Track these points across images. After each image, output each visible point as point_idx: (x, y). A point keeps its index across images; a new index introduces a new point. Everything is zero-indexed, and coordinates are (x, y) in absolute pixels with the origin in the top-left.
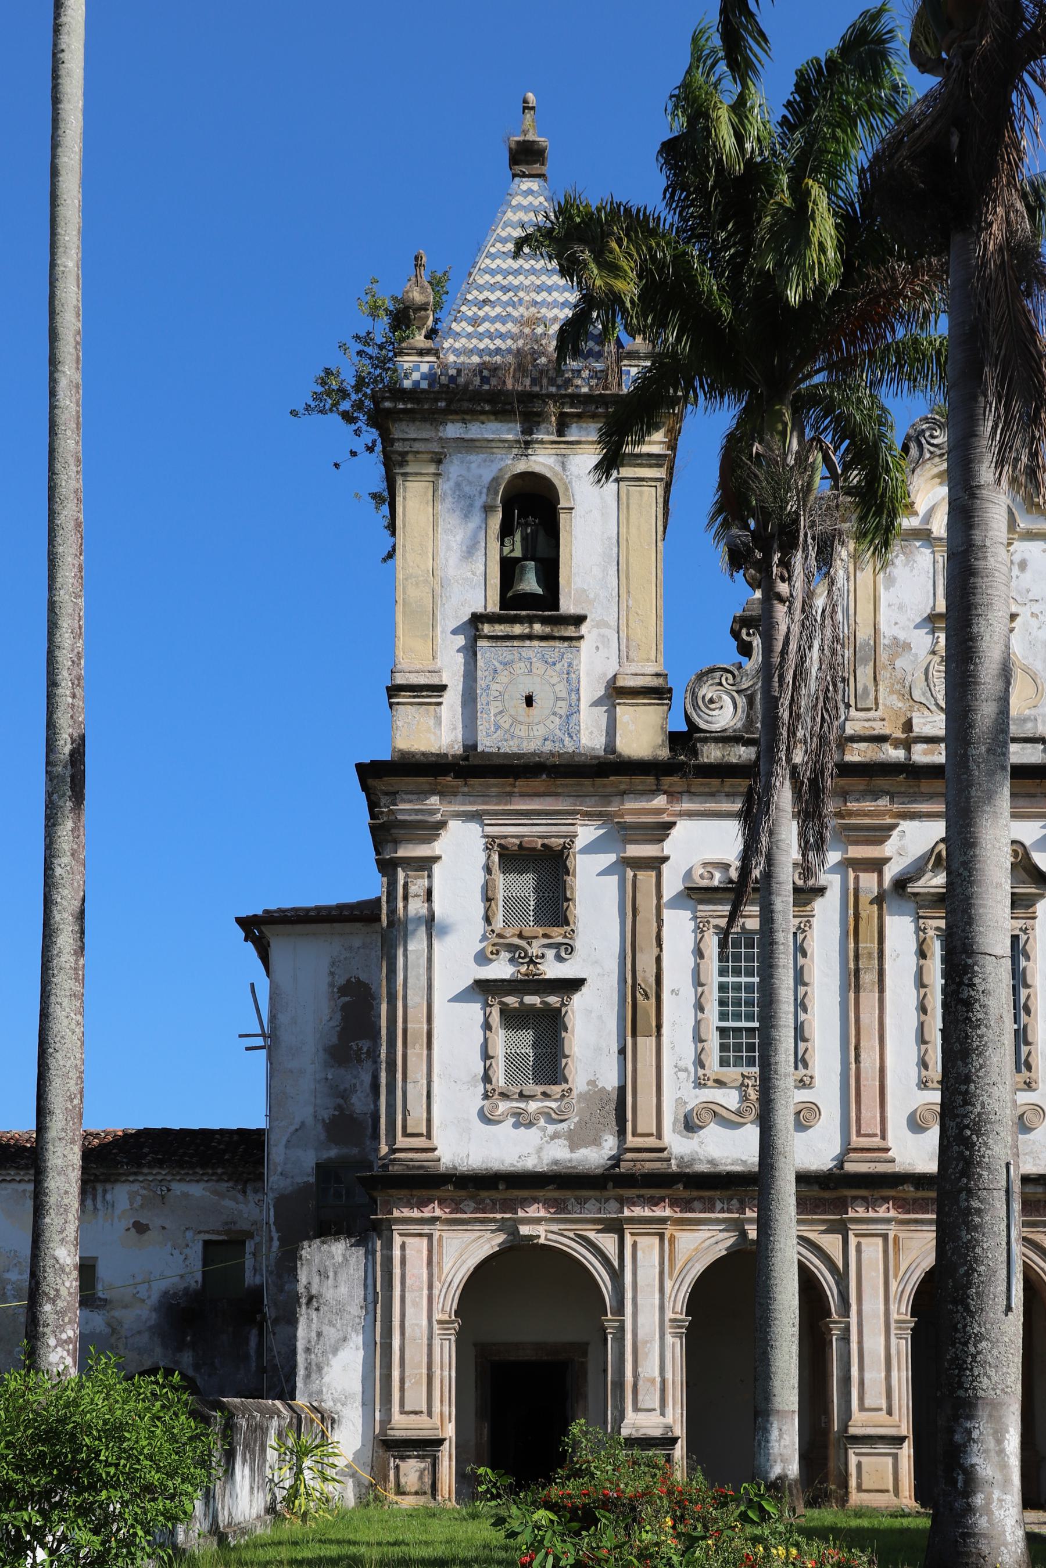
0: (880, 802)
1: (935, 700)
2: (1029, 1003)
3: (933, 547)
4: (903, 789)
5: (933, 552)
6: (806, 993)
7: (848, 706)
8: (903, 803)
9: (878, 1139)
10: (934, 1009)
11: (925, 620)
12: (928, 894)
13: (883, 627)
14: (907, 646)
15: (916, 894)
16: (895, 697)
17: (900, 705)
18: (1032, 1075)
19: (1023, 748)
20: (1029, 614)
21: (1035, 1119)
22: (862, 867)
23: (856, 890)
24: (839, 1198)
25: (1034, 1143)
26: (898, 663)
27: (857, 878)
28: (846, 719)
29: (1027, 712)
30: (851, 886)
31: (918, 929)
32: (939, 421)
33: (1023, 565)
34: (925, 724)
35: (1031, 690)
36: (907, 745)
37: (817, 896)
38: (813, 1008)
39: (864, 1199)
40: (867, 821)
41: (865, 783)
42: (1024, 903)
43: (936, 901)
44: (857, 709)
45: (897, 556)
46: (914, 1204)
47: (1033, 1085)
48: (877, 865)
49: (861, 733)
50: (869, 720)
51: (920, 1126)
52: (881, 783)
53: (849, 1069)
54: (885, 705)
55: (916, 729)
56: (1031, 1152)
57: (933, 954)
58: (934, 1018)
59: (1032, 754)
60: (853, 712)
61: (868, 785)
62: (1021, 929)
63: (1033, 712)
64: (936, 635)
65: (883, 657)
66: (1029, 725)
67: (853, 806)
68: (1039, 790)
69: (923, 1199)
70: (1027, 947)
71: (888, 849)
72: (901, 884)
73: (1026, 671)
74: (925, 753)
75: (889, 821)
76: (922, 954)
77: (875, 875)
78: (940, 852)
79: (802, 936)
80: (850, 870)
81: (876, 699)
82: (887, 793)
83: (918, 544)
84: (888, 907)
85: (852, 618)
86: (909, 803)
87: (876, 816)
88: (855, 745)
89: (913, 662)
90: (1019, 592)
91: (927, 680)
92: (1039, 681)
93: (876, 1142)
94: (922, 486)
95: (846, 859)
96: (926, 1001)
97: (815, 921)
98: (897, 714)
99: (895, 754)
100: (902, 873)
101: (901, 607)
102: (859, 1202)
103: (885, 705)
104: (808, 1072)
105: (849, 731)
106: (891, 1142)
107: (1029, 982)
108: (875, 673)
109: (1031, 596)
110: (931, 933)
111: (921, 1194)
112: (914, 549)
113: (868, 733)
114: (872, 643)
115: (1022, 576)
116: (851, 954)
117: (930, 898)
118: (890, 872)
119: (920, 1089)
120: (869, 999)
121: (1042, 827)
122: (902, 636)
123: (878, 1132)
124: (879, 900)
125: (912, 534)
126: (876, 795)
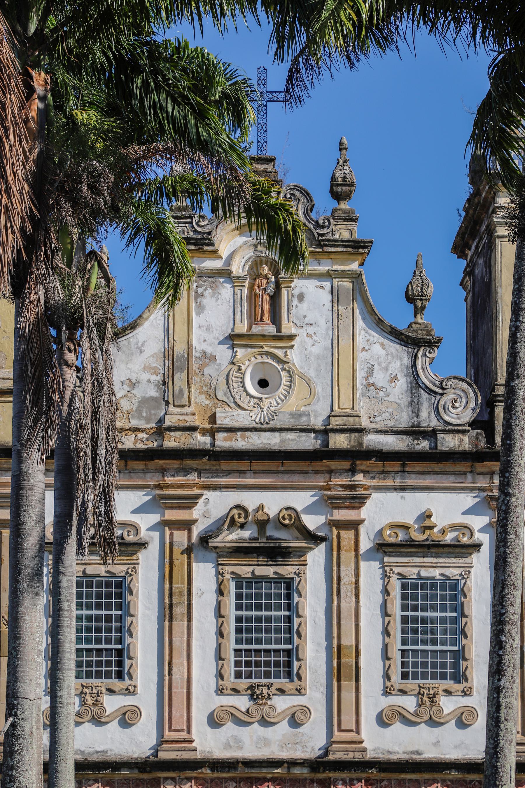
0: (190, 477)
2: (300, 629)
3: (234, 283)
4: (208, 467)
5: (233, 287)
6: (132, 622)
7: (167, 403)
8: (208, 478)
9: (184, 733)
10: (229, 633)
11: (226, 338)
12: (225, 547)
13: (195, 343)
14: (213, 358)
15: (216, 548)
17: (207, 402)
18: (302, 683)
19: (299, 437)
20: (305, 334)
21: (303, 717)
22: (176, 526)
23: (171, 544)
24: (154, 779)
25: (303, 735)
26: (206, 371)
27: (172, 535)
28: (166, 414)
29: (303, 408)
30: (168, 541)
31: (218, 573)
33: (301, 297)
34: (225, 418)
35: (306, 392)
36: (212, 432)
37: (141, 548)
38: (137, 633)
39: (173, 779)
40: (180, 492)
42: (298, 553)
43: (232, 552)
44: (174, 406)
45: (205, 290)
46: (211, 782)
47: (303, 691)
48: (187, 525)
49: (176, 424)
50: (183, 414)
51: (217, 723)
53: (163, 680)
54: (196, 403)
55: (219, 421)
56: (300, 742)
57: (229, 592)
58: (229, 641)
59: (306, 441)
60: (171, 408)
61: (180, 464)
62: (295, 573)
63: (308, 408)
64: (235, 350)
65: (195, 366)
66: (304, 419)
67: (169, 480)
68: (310, 468)
69: (219, 779)
70: (299, 587)
71: (196, 513)
72: (204, 540)
73: (303, 377)
74: (225, 440)
75: (197, 491)
76: (220, 592)
77: (186, 532)
79: (130, 579)
80: (167, 528)
81: (189, 398)
82: (196, 470)
83: (222, 280)
84: (195, 556)
85: (171, 336)
86: (212, 477)
87: (186, 488)
88: (172, 434)
89: (217, 370)
90: (298, 318)
91: (228, 383)
92: (312, 386)
93: (183, 735)
94: (225, 237)
95: (163, 520)
96: (222, 628)
97: (140, 568)
98: (205, 409)
99: (202, 441)
100: (206, 531)
101: (209, 328)
102: (169, 781)
103: (196, 403)
104: (133, 683)
105: (168, 422)
106: (194, 735)
107: (300, 613)
108: (188, 378)
109: (307, 321)
110: (228, 576)
111: (216, 775)
112: (219, 284)
113: (181, 424)
114: (186, 356)
115: (300, 305)
116: (167, 592)
117: (227, 550)
118: (196, 531)
119: (217, 694)
120: (180, 626)
123: (185, 728)
124: (188, 551)
125: (217, 273)
126: (186, 471)
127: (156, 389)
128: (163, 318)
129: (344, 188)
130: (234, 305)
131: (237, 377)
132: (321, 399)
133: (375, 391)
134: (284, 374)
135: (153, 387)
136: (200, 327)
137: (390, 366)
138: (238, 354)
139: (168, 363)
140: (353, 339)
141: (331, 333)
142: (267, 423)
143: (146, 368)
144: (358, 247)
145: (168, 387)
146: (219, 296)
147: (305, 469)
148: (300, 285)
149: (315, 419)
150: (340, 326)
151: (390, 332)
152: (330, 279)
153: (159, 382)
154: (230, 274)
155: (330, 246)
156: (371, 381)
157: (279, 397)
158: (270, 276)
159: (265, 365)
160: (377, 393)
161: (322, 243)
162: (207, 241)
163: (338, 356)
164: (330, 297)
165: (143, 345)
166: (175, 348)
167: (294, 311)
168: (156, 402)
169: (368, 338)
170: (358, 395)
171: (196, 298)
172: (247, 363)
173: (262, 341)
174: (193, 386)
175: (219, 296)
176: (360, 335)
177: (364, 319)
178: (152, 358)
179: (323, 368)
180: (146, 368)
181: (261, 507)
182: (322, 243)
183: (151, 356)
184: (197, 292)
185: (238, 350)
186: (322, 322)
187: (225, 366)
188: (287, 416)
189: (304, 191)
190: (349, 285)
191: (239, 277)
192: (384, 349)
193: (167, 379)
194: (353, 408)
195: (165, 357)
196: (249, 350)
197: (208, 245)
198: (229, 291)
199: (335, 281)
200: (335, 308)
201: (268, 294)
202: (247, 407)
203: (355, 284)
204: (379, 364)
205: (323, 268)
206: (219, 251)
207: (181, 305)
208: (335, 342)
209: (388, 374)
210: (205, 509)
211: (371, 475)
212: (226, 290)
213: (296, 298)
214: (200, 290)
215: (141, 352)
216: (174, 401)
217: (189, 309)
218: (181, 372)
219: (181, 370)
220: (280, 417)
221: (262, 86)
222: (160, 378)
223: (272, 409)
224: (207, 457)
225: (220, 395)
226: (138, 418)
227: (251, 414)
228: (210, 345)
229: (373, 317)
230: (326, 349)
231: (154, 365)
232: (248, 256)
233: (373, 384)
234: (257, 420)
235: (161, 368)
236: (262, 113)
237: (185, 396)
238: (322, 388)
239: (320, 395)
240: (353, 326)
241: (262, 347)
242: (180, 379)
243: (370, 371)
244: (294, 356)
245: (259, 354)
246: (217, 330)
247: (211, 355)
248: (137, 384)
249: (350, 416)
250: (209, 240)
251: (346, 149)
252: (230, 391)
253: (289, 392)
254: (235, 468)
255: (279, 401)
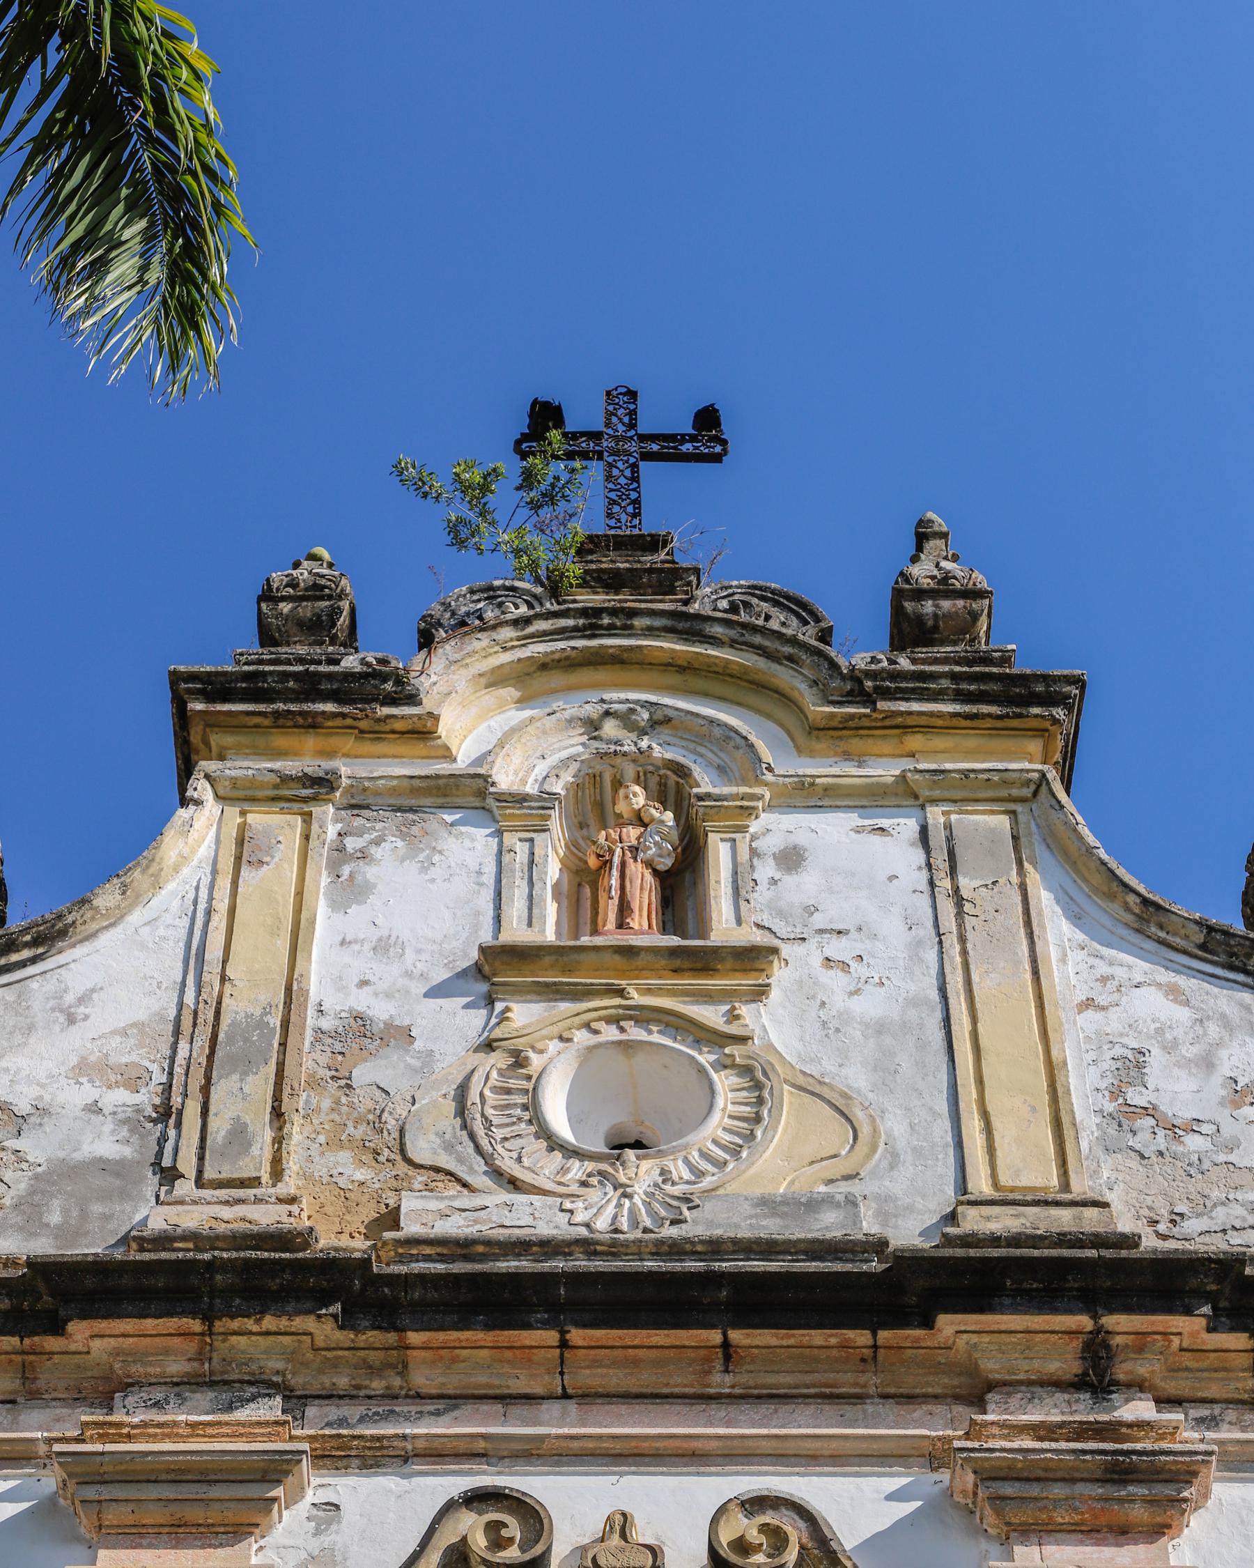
1: (488, 1159)
4: (343, 1382)
5: (499, 833)
7: (170, 1175)
8: (342, 1422)
11: (463, 974)
13: (318, 982)
16: (345, 1156)
20: (817, 961)
26: (363, 1074)
29: (822, 1189)
32: (528, 592)
33: (791, 859)
35: (833, 1135)
41: (192, 1347)
44: (200, 1183)
45: (377, 842)
52: (255, 1339)
54: (305, 1176)
61: (200, 1357)
63: (844, 1187)
64: (499, 1006)
65: (309, 1060)
68: (872, 1381)
78: (464, 1539)
83: (449, 818)
86: (362, 1420)
90: (781, 914)
91: (461, 1111)
92: (859, 1115)
101: (382, 947)
108: (277, 1098)
109: (819, 921)
114: (275, 1021)
115: (789, 880)
121: (891, 1497)
122: (381, 1011)
127: (124, 1132)
128: (186, 922)
129: (946, 604)
130: (499, 881)
131: (508, 1091)
132: (907, 1157)
133: (1161, 1133)
134: (724, 1082)
135: (109, 1127)
136: (343, 943)
137: (1223, 1053)
138: (508, 1014)
139: (192, 1050)
140: (1036, 973)
141: (931, 956)
142: (646, 1230)
143: (82, 1070)
144: (1020, 697)
145: (178, 1125)
146: (436, 858)
147: (847, 1381)
148: (784, 827)
149: (884, 1224)
150: (970, 935)
151: (1203, 947)
152: (918, 811)
153: (138, 1111)
154: (482, 794)
155: (906, 695)
156: (1137, 1097)
157: (704, 1155)
158: (656, 814)
159: (640, 1059)
160: (1177, 1138)
161: (869, 684)
162: (389, 686)
163: (974, 1020)
164: (919, 856)
165: (81, 1000)
166: (226, 1000)
167: (762, 895)
168: (118, 1175)
169: (1103, 969)
170: (1084, 1145)
171: (334, 869)
172: (553, 1046)
173: (623, 974)
174: (297, 1119)
175: (436, 858)
176: (1063, 959)
177: (1076, 918)
178: (118, 1039)
179: (905, 1063)
180: (82, 1070)
181: (621, 1524)
182: (869, 684)
183: (114, 1032)
184: (341, 849)
185: (513, 1005)
186: (892, 928)
187: (449, 1060)
188: (747, 1208)
189: (788, 597)
190: (1003, 822)
191: (521, 799)
192: (1187, 1003)
193: (176, 1100)
194: (1065, 1186)
195: (177, 1033)
196: (565, 1007)
197: (392, 701)
198: (479, 846)
199: (936, 815)
200: (945, 884)
201: (648, 864)
202: (549, 1186)
203: (1022, 818)
204: (1170, 1047)
205: (885, 770)
206: (442, 730)
207: (270, 882)
208: (955, 982)
209: (1217, 1080)
210: (314, 1545)
211: (1194, 1413)
212: (468, 846)
213: (771, 861)
214: (351, 843)
215: (71, 1020)
216: (200, 1172)
217: (300, 894)
218: (246, 1074)
219: (246, 1064)
220: (709, 1209)
221: (621, 428)
222: (147, 1098)
223: (677, 1190)
224: (337, 1308)
225: (423, 1148)
226: (21, 1229)
227: (568, 1205)
228: (388, 995)
229: (1116, 908)
230: (914, 1002)
231: (124, 1060)
232: (564, 754)
233: (1148, 1111)
234: (602, 1224)
235: (155, 1068)
236: (622, 481)
237: (255, 1150)
238: (909, 1120)
239: (901, 1145)
240: (1030, 935)
241: (620, 993)
242: (240, 1098)
243: (1132, 1067)
244: (774, 1024)
245: (614, 1020)
246: (419, 951)
247: (389, 1026)
248: (33, 1120)
249: (1057, 1204)
250: (399, 682)
251: (944, 536)
252: (472, 1136)
253: (751, 1136)
254: (481, 1380)
255: (705, 1165)
